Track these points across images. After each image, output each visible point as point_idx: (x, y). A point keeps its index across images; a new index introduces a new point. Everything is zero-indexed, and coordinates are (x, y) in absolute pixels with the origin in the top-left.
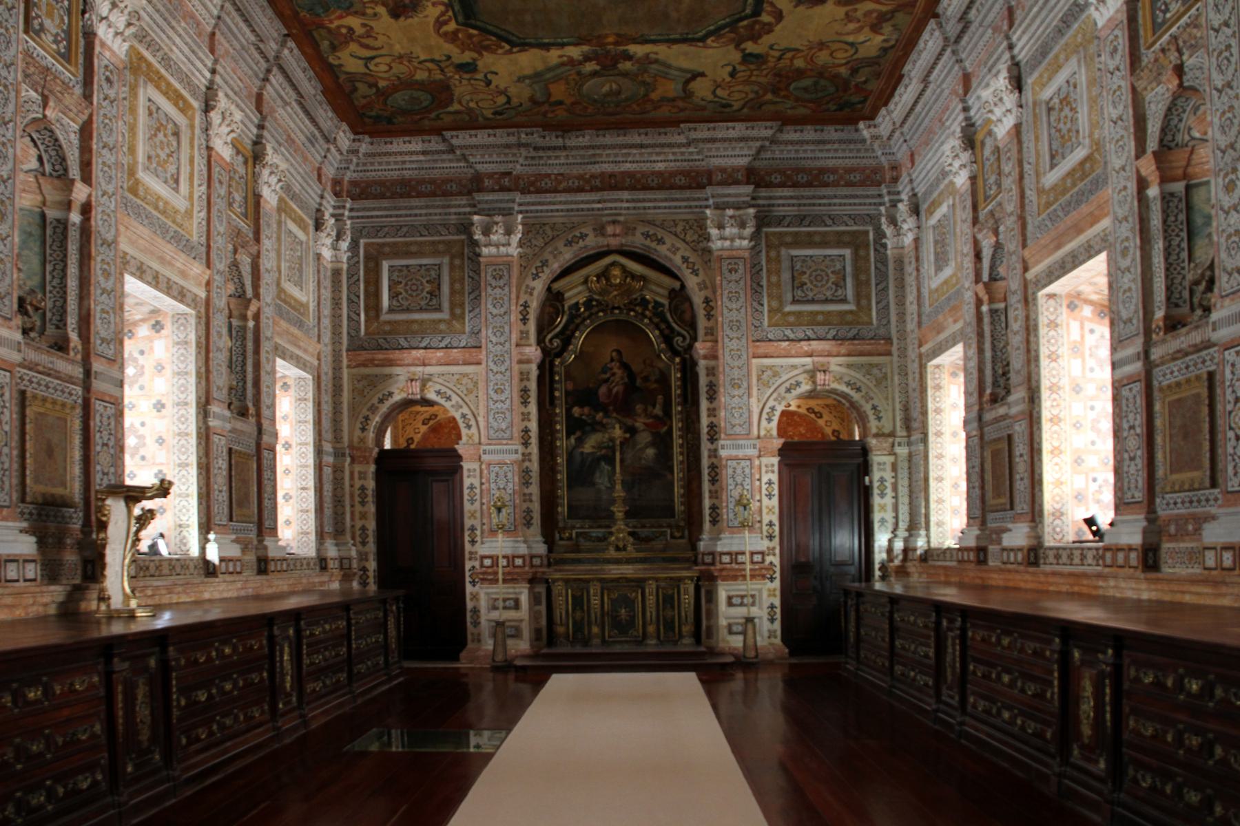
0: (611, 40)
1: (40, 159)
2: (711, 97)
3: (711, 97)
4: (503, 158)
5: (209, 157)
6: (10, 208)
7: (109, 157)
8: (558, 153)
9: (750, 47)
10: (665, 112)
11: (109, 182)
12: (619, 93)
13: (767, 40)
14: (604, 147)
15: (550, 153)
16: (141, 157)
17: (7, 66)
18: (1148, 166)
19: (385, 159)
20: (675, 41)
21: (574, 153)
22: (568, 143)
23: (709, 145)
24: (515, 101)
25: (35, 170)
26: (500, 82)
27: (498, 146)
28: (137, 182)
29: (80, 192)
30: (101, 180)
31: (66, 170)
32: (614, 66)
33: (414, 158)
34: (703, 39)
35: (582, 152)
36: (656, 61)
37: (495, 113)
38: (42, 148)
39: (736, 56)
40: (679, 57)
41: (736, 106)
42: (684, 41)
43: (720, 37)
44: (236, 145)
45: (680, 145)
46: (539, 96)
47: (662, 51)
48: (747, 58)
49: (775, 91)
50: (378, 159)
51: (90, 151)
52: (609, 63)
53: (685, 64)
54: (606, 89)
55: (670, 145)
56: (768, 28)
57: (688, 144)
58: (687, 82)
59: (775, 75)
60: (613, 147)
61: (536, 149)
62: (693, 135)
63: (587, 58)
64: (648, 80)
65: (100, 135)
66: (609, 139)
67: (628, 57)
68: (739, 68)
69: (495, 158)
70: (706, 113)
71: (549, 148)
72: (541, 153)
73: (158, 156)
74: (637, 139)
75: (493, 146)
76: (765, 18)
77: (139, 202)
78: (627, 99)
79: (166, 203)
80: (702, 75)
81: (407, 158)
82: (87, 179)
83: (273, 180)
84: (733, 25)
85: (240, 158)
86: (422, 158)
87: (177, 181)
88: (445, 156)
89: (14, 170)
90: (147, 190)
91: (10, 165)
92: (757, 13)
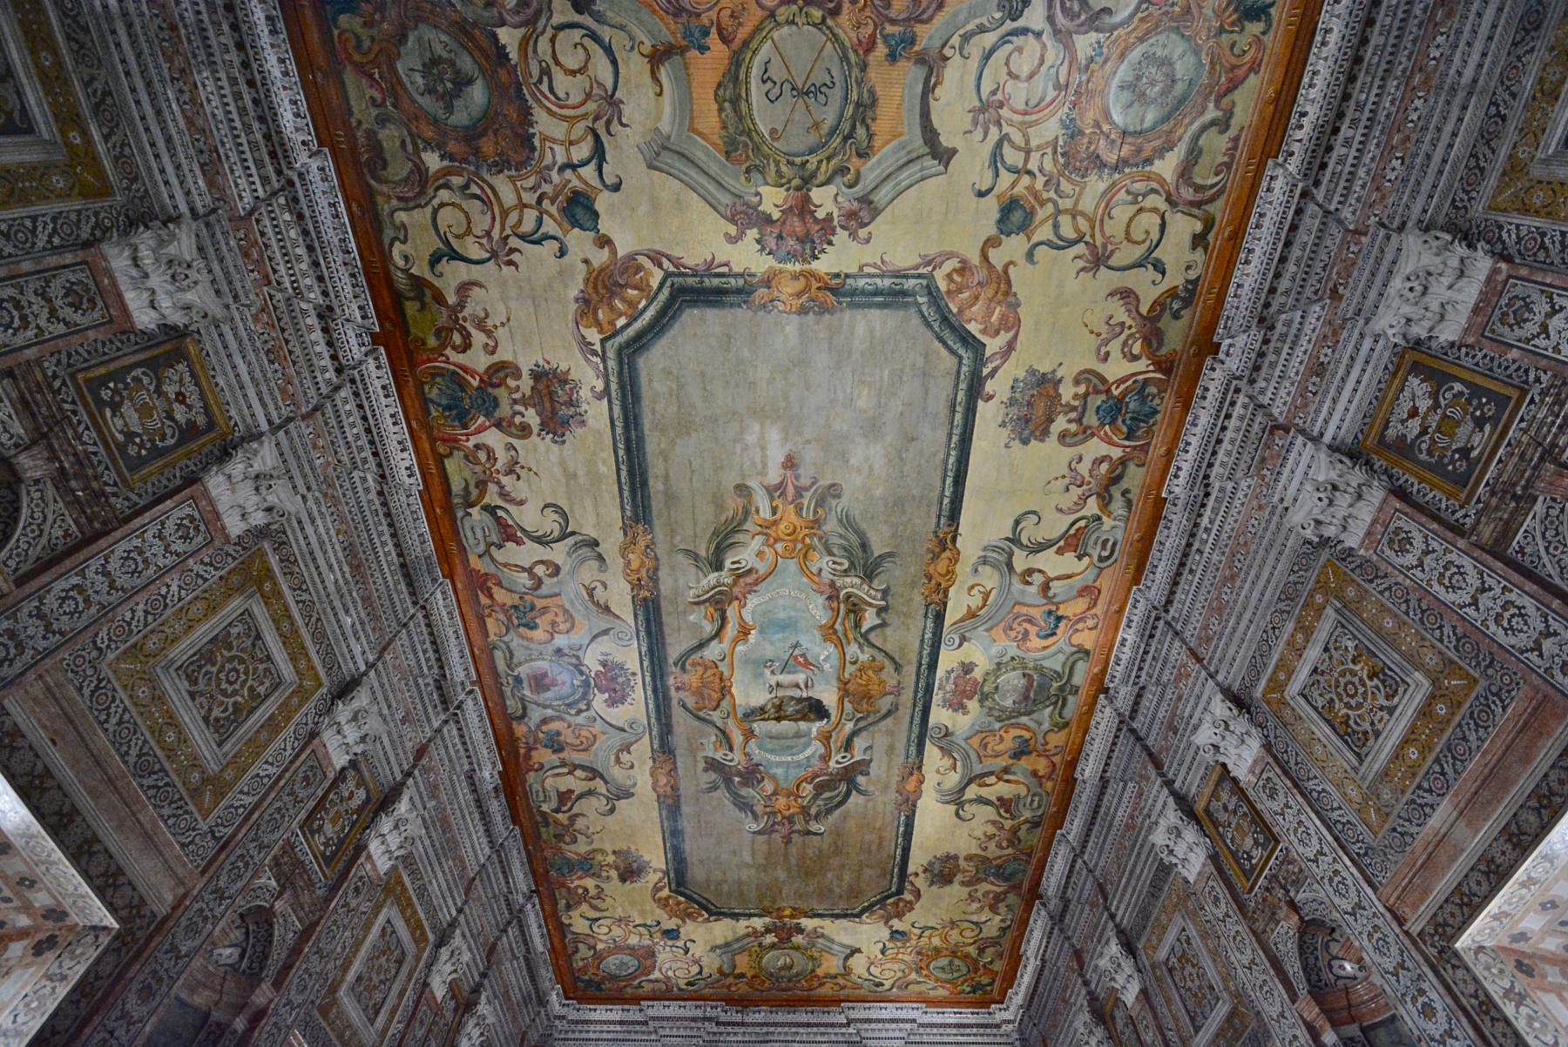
0: (787, 912)
1: (242, 956)
2: (866, 975)
3: (866, 975)
4: (689, 1033)
5: (422, 993)
6: (164, 988)
7: (315, 964)
8: (737, 1029)
9: (897, 924)
10: (827, 990)
11: (302, 992)
12: (791, 967)
13: (910, 917)
14: (775, 1024)
15: (729, 1029)
16: (351, 976)
17: (261, 847)
18: (1312, 1012)
19: (586, 1027)
20: (837, 916)
21: (750, 1030)
22: (748, 1019)
23: (866, 1026)
24: (706, 972)
25: (231, 965)
26: (697, 950)
27: (686, 1019)
28: (335, 1002)
29: (263, 995)
30: (294, 987)
31: (262, 969)
32: (789, 939)
33: (612, 1028)
34: (859, 915)
35: (757, 1029)
36: (823, 935)
37: (689, 984)
38: (251, 941)
39: (886, 933)
40: (841, 932)
41: (888, 984)
42: (845, 916)
43: (873, 913)
44: (453, 988)
45: (841, 1025)
46: (726, 969)
47: (829, 926)
48: (896, 935)
49: (919, 970)
50: (579, 1027)
51: (300, 952)
52: (785, 934)
53: (846, 940)
54: (780, 963)
55: (832, 1025)
56: (910, 906)
57: (848, 1024)
58: (847, 958)
59: (919, 953)
60: (783, 1025)
61: (718, 1024)
62: (854, 1015)
63: (768, 931)
64: (816, 955)
65: (318, 939)
66: (780, 1017)
67: (800, 930)
68: (889, 945)
69: (682, 1032)
70: (862, 992)
71: (729, 1024)
72: (722, 1029)
73: (370, 979)
74: (804, 1018)
75: (681, 1019)
76: (907, 896)
77: (324, 1024)
78: (798, 974)
79: (354, 1034)
80: (858, 951)
81: (605, 1028)
82: (277, 984)
83: (476, 1033)
84: (882, 901)
85: (453, 1004)
86: (618, 1028)
87: (377, 1013)
88: (638, 1028)
89: (197, 950)
90: (341, 1013)
91: (197, 943)
92: (900, 891)
